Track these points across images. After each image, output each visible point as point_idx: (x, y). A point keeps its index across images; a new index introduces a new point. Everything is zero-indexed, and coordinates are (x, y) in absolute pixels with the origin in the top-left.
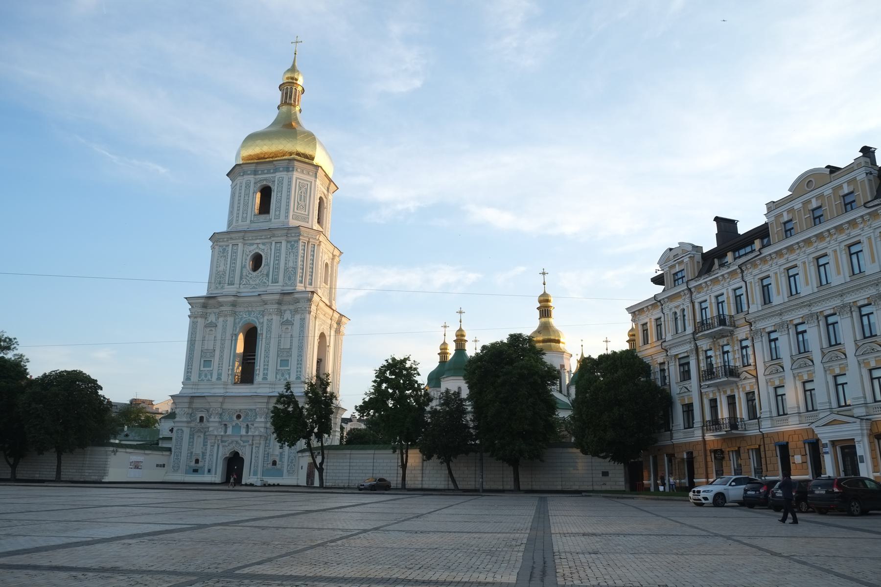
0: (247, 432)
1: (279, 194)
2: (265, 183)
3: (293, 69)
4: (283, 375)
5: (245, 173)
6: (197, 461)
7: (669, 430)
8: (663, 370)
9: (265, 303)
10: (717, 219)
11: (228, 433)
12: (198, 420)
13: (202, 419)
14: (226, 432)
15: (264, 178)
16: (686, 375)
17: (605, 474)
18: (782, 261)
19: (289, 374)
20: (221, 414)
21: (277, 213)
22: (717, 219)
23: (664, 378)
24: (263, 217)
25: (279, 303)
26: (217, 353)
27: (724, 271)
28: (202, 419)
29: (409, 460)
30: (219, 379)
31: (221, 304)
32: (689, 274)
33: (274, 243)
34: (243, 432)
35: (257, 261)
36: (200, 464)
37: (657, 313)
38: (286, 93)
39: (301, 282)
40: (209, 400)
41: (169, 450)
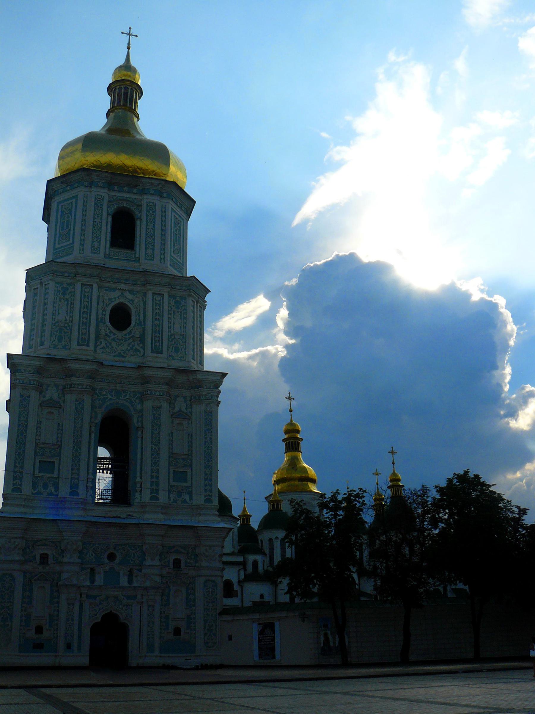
0: (130, 582)
1: (151, 226)
2: (124, 204)
6: (39, 630)
9: (145, 380)
11: (96, 583)
13: (44, 558)
14: (92, 581)
15: (125, 197)
19: (190, 494)
21: (150, 251)
24: (122, 253)
30: (74, 493)
34: (124, 581)
35: (120, 317)
36: (46, 634)
38: (126, 94)
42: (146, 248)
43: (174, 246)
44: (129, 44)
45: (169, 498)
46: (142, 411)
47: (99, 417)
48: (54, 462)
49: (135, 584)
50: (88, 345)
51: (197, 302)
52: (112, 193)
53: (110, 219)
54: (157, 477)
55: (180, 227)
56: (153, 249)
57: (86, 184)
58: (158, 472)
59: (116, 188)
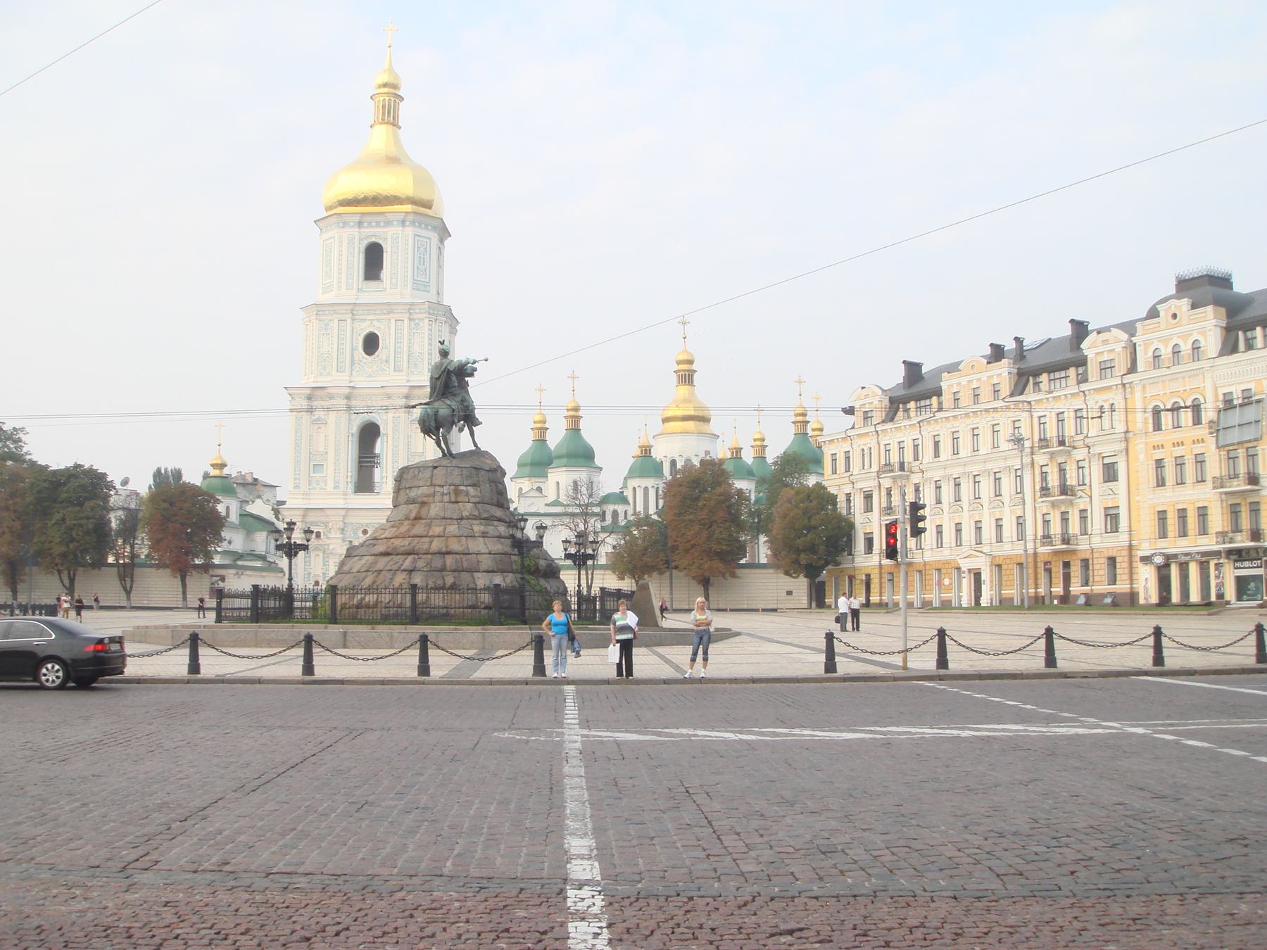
2: (373, 240)
5: (345, 224)
7: (850, 554)
8: (848, 500)
10: (904, 362)
16: (868, 509)
17: (789, 593)
18: (949, 425)
21: (394, 281)
22: (904, 362)
23: (849, 508)
24: (373, 285)
26: (331, 455)
27: (907, 423)
31: (331, 397)
32: (878, 416)
33: (393, 322)
35: (371, 343)
37: (846, 446)
40: (328, 512)
53: (362, 257)
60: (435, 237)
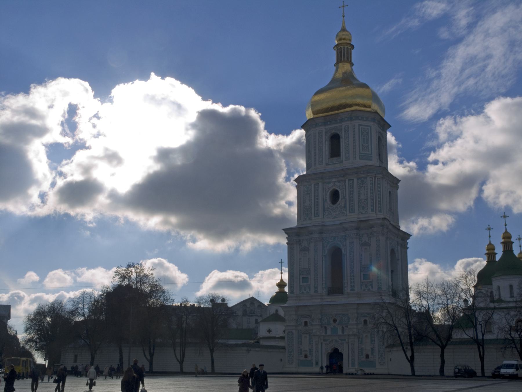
0: (343, 332)
2: (334, 131)
3: (344, 30)
4: (366, 286)
6: (306, 356)
11: (328, 334)
12: (303, 324)
13: (306, 323)
19: (372, 285)
20: (321, 319)
24: (335, 159)
25: (357, 229)
28: (306, 323)
29: (486, 353)
30: (316, 291)
34: (340, 332)
35: (335, 196)
36: (309, 358)
38: (341, 52)
39: (372, 210)
41: (284, 348)
42: (345, 154)
43: (363, 146)
44: (343, 13)
45: (361, 288)
46: (346, 245)
47: (326, 252)
48: (308, 277)
49: (345, 334)
50: (319, 216)
51: (375, 177)
52: (327, 127)
54: (354, 279)
55: (368, 133)
56: (349, 153)
57: (314, 126)
58: (354, 276)
59: (329, 123)
60: (374, 128)
